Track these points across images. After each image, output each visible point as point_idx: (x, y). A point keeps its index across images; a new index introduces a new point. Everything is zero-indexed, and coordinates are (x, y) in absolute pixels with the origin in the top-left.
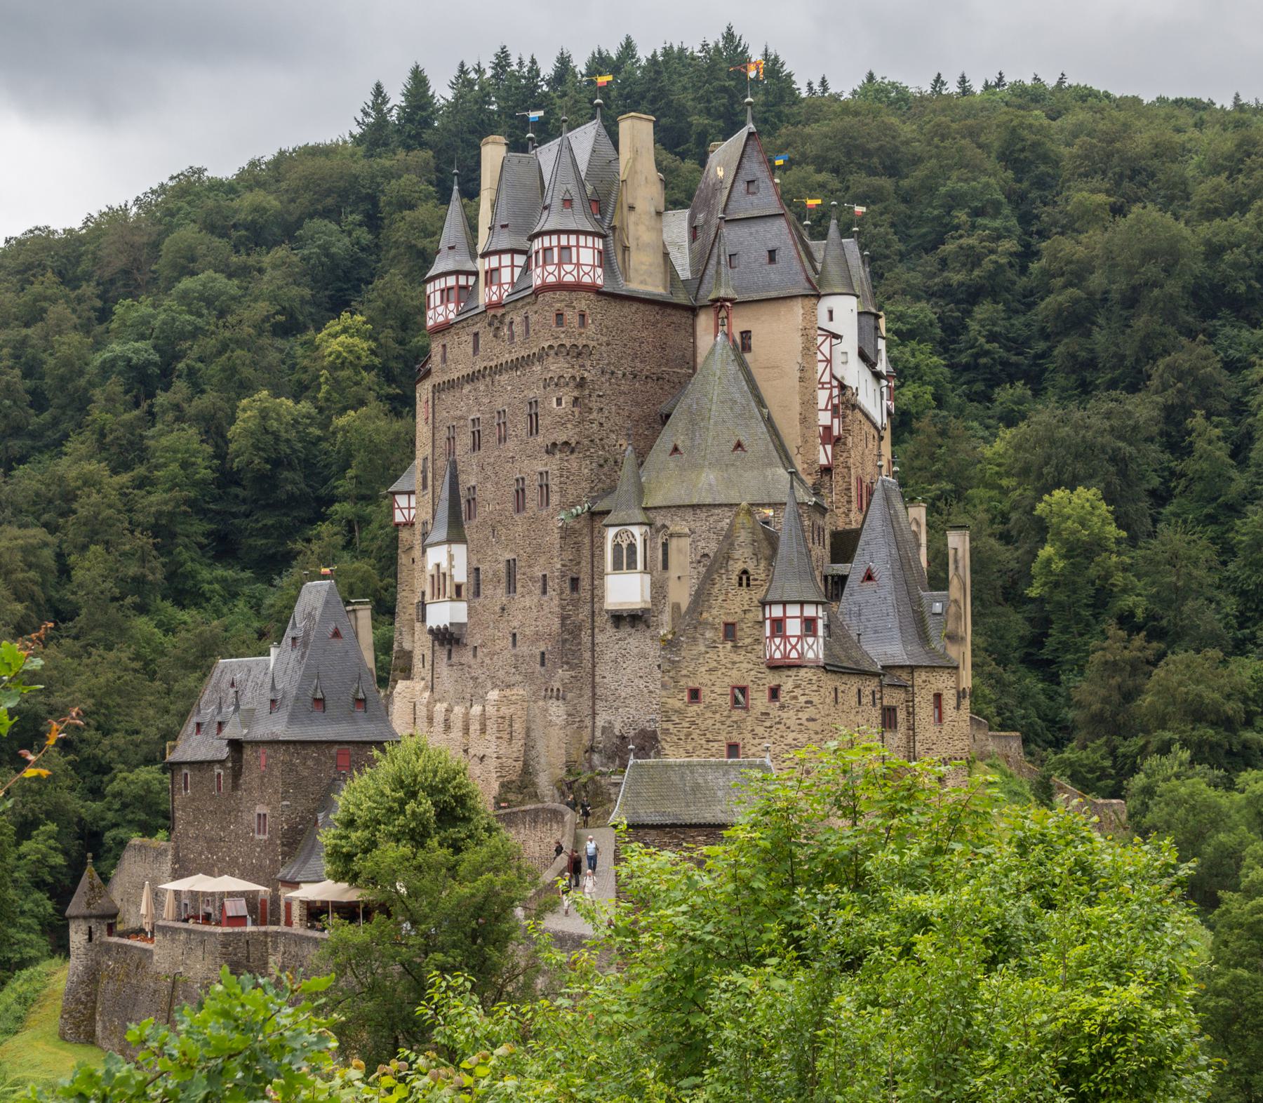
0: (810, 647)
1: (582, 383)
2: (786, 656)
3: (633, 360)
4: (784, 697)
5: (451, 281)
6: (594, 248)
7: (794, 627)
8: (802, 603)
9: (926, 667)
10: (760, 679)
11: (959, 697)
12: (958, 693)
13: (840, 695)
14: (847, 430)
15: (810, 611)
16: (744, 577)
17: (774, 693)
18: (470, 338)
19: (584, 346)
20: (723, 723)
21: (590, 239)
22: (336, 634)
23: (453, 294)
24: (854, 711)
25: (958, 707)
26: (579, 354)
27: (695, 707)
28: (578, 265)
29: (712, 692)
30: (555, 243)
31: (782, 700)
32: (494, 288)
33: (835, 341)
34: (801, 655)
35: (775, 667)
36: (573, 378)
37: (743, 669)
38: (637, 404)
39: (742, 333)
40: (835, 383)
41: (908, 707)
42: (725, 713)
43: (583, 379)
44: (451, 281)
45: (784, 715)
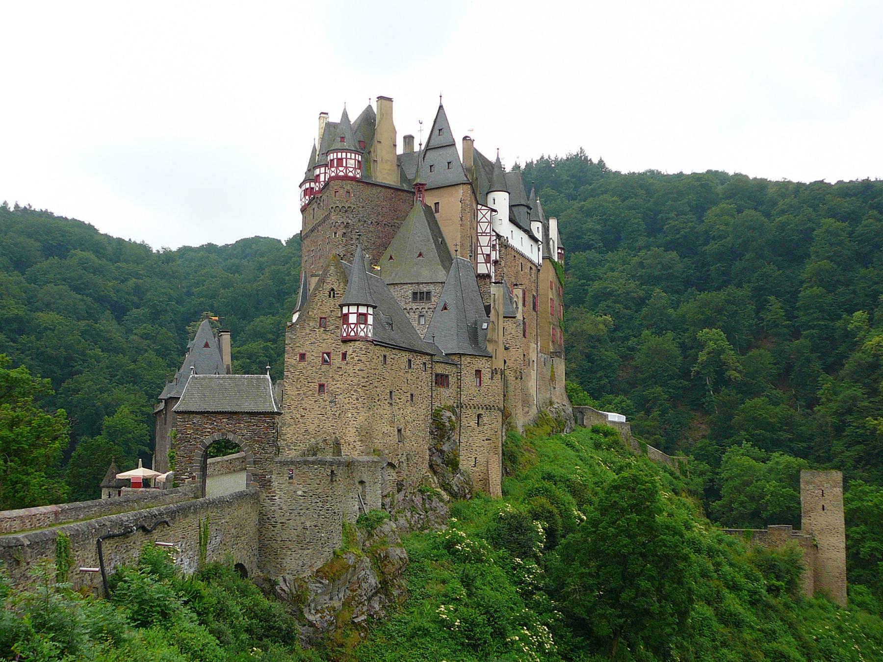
0: (362, 330)
2: (348, 335)
3: (377, 216)
4: (348, 358)
5: (307, 185)
6: (355, 159)
7: (353, 319)
8: (358, 305)
9: (470, 355)
10: (338, 348)
11: (492, 373)
12: (492, 370)
13: (388, 360)
14: (500, 257)
15: (363, 310)
16: (332, 292)
17: (344, 355)
18: (312, 211)
19: (349, 207)
20: (317, 373)
21: (353, 155)
22: (207, 345)
23: (308, 192)
24: (403, 371)
25: (492, 379)
27: (302, 364)
28: (346, 167)
29: (312, 355)
30: (335, 157)
31: (347, 359)
32: (317, 184)
33: (494, 213)
34: (356, 334)
35: (345, 341)
36: (343, 222)
37: (329, 342)
38: (379, 237)
39: (436, 204)
40: (494, 234)
41: (457, 375)
42: (318, 368)
44: (307, 185)
45: (348, 368)
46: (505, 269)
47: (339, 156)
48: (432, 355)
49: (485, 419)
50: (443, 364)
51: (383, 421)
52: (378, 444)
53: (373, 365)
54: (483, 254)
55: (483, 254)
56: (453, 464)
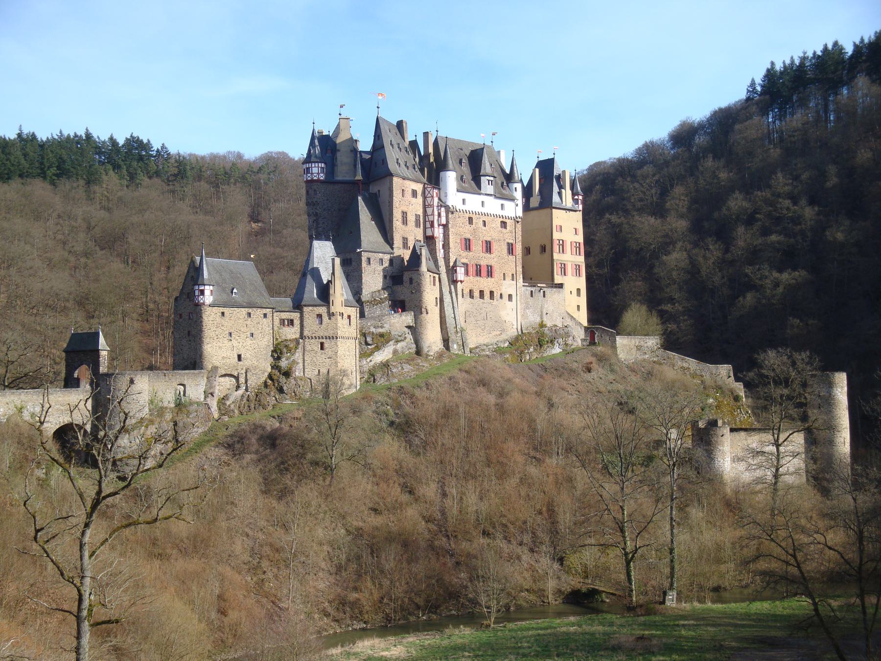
0: (202, 299)
1: (316, 215)
6: (318, 167)
7: (197, 293)
8: (199, 285)
14: (447, 221)
15: (202, 288)
26: (314, 205)
27: (181, 320)
28: (312, 174)
43: (316, 213)
46: (451, 230)
47: (308, 166)
48: (273, 308)
49: (326, 345)
50: (288, 313)
51: (222, 350)
52: (217, 364)
53: (211, 319)
54: (429, 221)
55: (429, 221)
56: (287, 374)
